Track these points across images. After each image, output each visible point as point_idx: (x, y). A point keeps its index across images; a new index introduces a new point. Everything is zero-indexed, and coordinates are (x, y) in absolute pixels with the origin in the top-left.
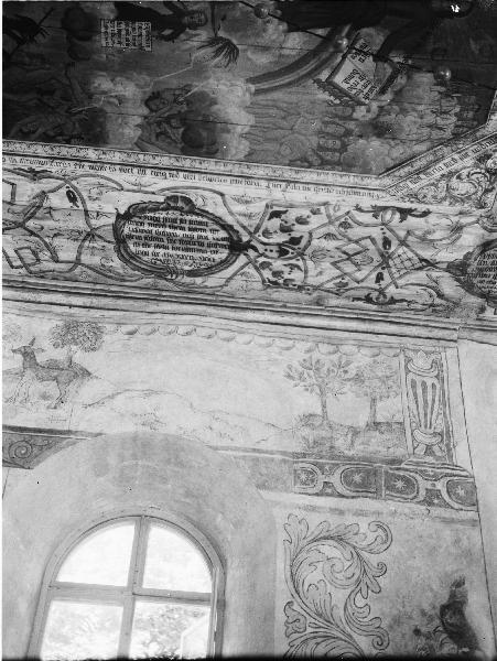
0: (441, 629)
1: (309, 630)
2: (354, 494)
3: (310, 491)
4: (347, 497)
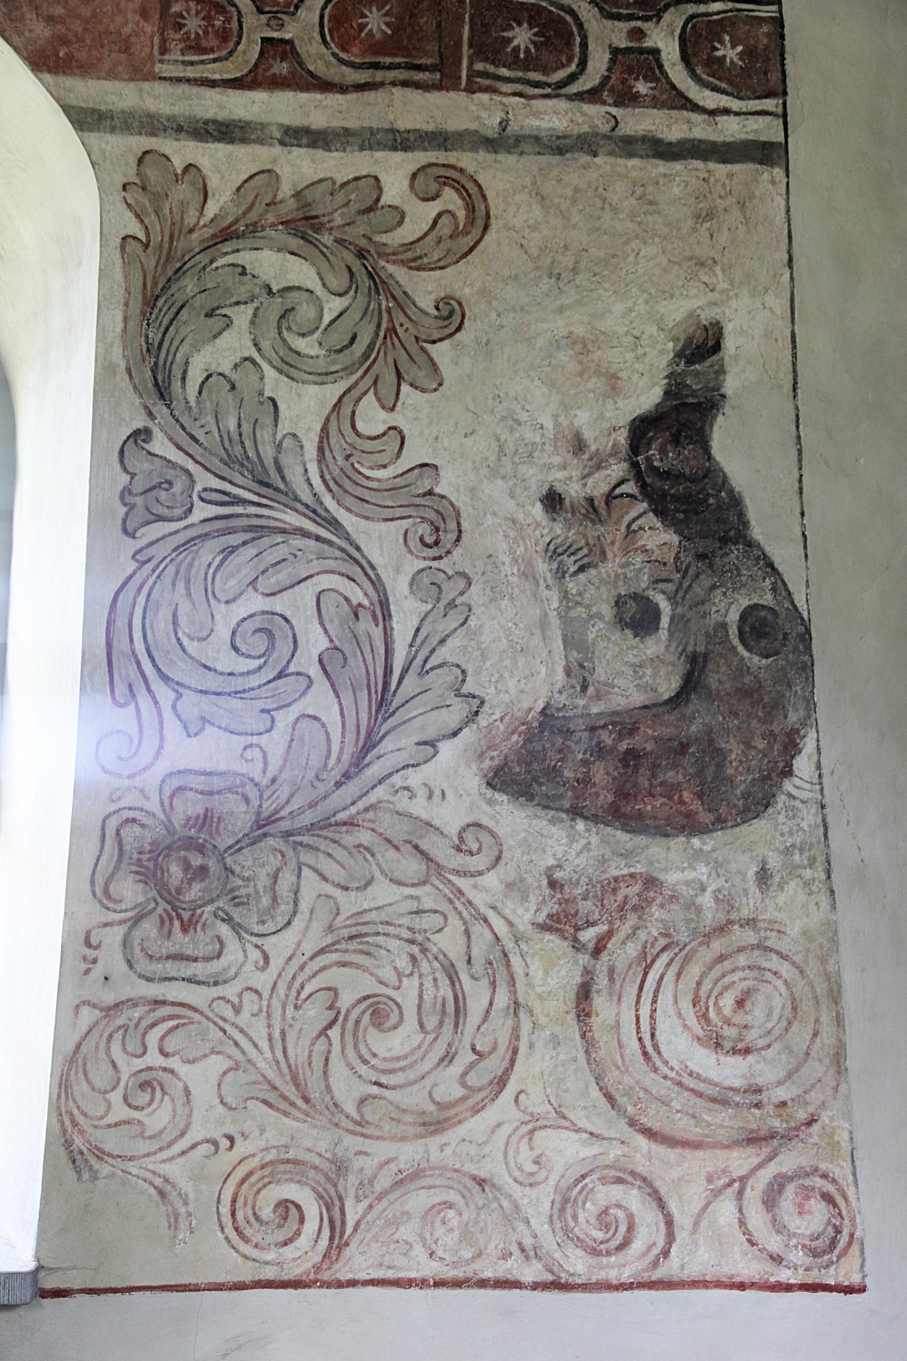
0: (630, 487)
1: (202, 511)
2: (363, 76)
3: (214, 72)
4: (343, 89)
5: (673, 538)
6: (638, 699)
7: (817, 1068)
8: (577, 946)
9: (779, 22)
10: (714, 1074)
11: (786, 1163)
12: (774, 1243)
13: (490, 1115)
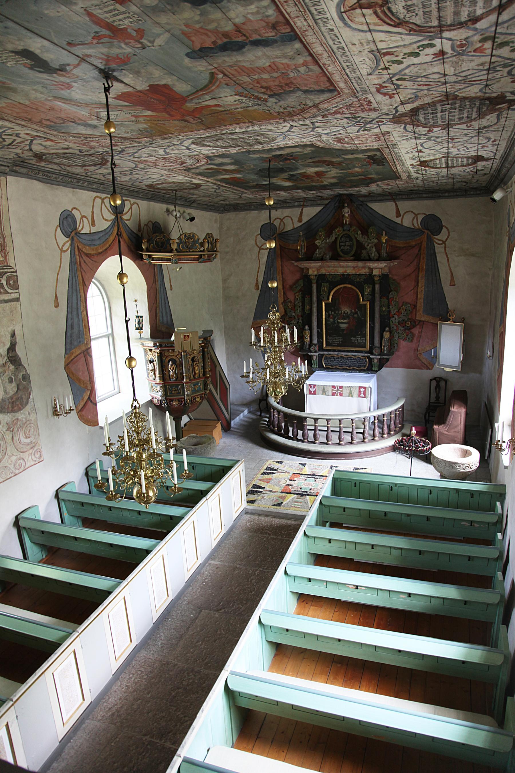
0: (8, 360)
5: (13, 367)
6: (13, 393)
7: (37, 436)
8: (11, 431)
9: (17, 276)
10: (27, 442)
11: (35, 449)
12: (35, 459)
13: (5, 458)
